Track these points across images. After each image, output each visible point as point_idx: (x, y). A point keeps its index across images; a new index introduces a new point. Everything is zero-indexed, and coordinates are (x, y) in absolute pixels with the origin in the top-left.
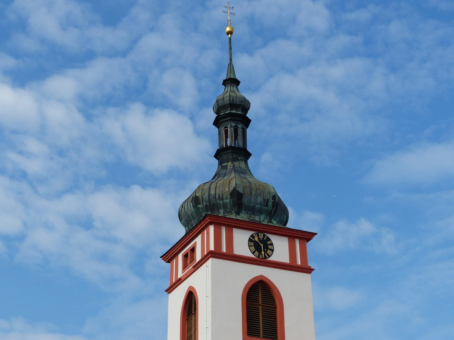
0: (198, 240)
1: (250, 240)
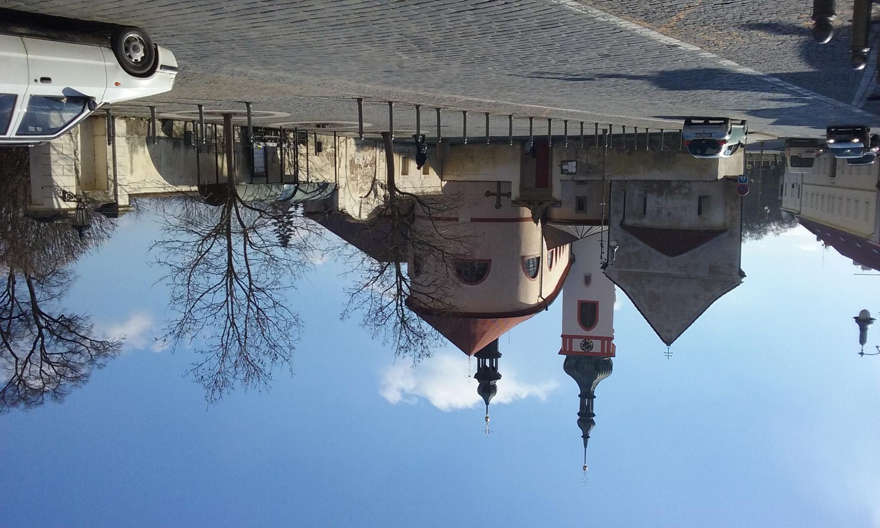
1: (592, 347)
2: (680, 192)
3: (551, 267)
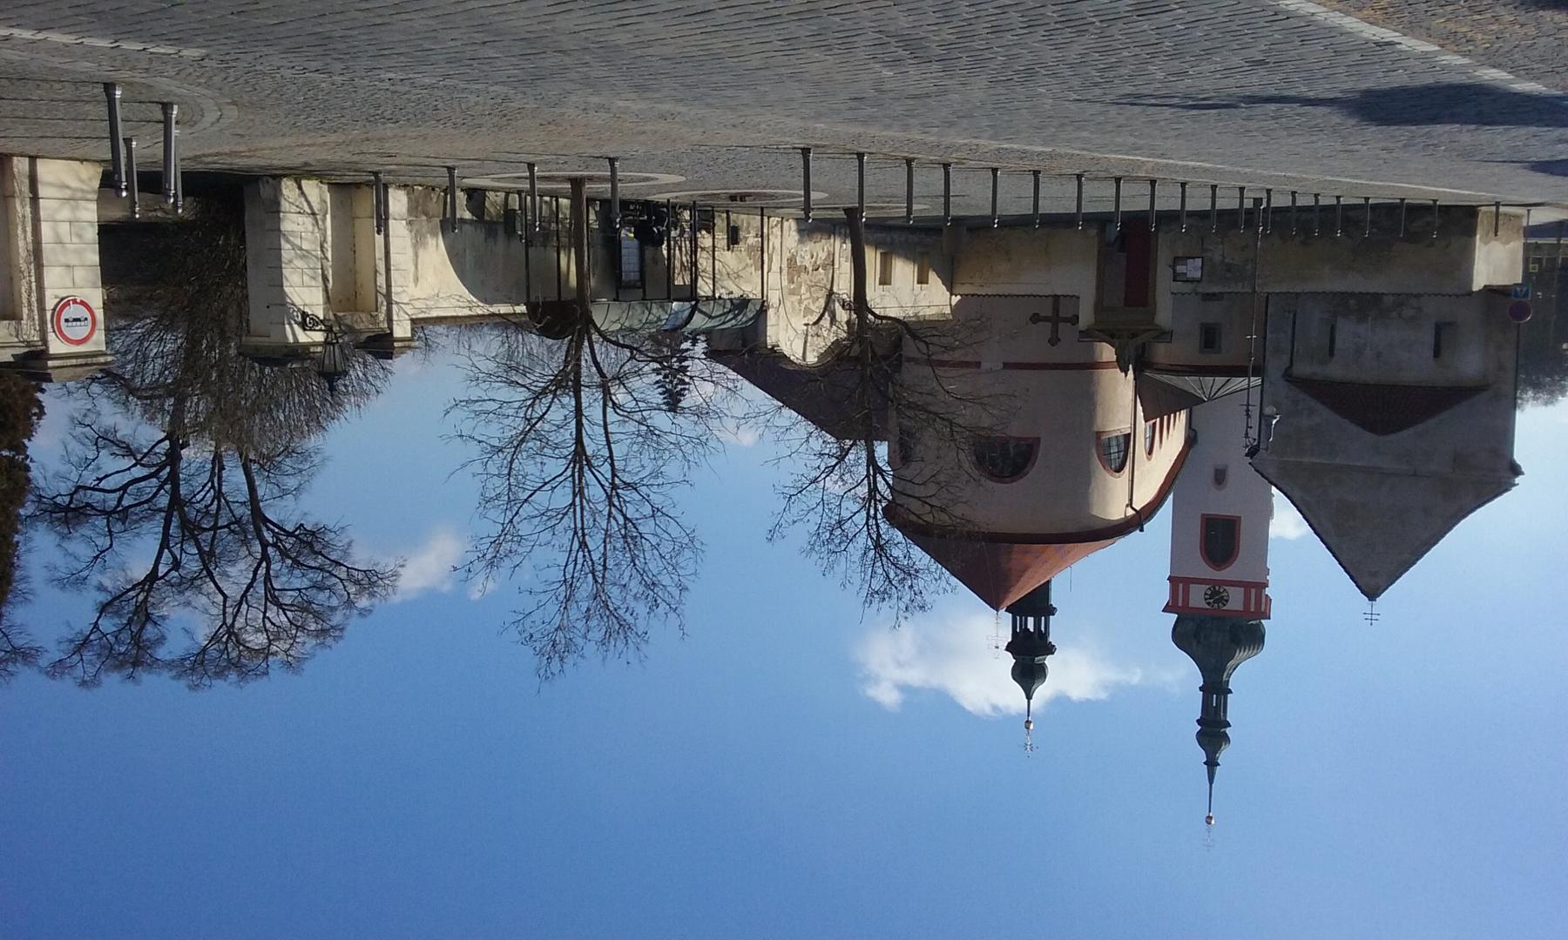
1: (1227, 601)
2: (1400, 316)
3: (1150, 452)
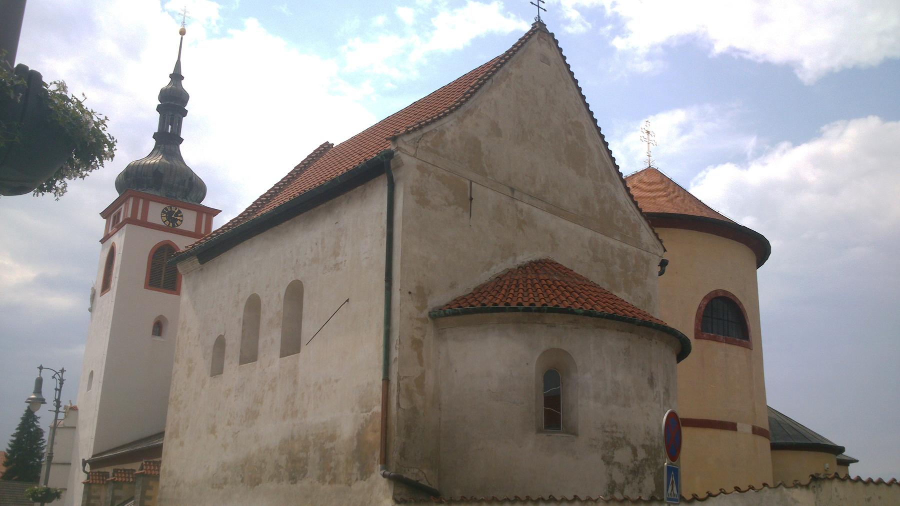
0: (123, 207)
1: (163, 212)
2: (634, 452)
